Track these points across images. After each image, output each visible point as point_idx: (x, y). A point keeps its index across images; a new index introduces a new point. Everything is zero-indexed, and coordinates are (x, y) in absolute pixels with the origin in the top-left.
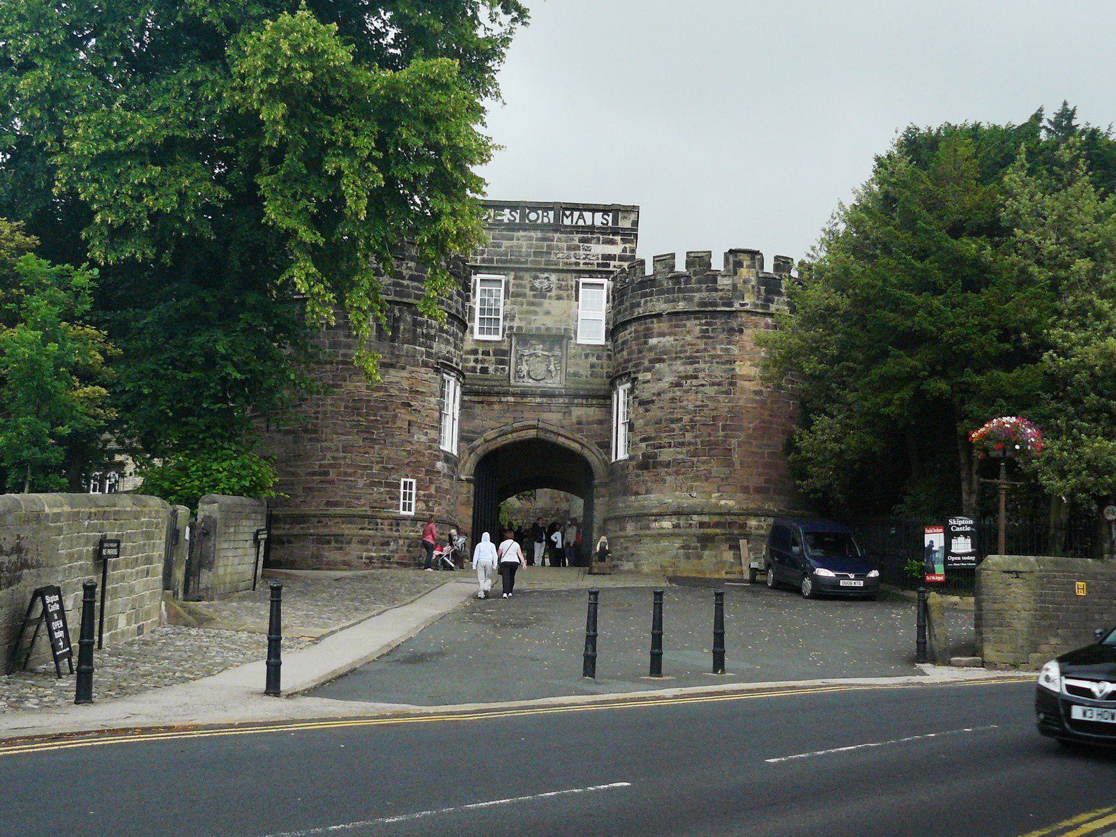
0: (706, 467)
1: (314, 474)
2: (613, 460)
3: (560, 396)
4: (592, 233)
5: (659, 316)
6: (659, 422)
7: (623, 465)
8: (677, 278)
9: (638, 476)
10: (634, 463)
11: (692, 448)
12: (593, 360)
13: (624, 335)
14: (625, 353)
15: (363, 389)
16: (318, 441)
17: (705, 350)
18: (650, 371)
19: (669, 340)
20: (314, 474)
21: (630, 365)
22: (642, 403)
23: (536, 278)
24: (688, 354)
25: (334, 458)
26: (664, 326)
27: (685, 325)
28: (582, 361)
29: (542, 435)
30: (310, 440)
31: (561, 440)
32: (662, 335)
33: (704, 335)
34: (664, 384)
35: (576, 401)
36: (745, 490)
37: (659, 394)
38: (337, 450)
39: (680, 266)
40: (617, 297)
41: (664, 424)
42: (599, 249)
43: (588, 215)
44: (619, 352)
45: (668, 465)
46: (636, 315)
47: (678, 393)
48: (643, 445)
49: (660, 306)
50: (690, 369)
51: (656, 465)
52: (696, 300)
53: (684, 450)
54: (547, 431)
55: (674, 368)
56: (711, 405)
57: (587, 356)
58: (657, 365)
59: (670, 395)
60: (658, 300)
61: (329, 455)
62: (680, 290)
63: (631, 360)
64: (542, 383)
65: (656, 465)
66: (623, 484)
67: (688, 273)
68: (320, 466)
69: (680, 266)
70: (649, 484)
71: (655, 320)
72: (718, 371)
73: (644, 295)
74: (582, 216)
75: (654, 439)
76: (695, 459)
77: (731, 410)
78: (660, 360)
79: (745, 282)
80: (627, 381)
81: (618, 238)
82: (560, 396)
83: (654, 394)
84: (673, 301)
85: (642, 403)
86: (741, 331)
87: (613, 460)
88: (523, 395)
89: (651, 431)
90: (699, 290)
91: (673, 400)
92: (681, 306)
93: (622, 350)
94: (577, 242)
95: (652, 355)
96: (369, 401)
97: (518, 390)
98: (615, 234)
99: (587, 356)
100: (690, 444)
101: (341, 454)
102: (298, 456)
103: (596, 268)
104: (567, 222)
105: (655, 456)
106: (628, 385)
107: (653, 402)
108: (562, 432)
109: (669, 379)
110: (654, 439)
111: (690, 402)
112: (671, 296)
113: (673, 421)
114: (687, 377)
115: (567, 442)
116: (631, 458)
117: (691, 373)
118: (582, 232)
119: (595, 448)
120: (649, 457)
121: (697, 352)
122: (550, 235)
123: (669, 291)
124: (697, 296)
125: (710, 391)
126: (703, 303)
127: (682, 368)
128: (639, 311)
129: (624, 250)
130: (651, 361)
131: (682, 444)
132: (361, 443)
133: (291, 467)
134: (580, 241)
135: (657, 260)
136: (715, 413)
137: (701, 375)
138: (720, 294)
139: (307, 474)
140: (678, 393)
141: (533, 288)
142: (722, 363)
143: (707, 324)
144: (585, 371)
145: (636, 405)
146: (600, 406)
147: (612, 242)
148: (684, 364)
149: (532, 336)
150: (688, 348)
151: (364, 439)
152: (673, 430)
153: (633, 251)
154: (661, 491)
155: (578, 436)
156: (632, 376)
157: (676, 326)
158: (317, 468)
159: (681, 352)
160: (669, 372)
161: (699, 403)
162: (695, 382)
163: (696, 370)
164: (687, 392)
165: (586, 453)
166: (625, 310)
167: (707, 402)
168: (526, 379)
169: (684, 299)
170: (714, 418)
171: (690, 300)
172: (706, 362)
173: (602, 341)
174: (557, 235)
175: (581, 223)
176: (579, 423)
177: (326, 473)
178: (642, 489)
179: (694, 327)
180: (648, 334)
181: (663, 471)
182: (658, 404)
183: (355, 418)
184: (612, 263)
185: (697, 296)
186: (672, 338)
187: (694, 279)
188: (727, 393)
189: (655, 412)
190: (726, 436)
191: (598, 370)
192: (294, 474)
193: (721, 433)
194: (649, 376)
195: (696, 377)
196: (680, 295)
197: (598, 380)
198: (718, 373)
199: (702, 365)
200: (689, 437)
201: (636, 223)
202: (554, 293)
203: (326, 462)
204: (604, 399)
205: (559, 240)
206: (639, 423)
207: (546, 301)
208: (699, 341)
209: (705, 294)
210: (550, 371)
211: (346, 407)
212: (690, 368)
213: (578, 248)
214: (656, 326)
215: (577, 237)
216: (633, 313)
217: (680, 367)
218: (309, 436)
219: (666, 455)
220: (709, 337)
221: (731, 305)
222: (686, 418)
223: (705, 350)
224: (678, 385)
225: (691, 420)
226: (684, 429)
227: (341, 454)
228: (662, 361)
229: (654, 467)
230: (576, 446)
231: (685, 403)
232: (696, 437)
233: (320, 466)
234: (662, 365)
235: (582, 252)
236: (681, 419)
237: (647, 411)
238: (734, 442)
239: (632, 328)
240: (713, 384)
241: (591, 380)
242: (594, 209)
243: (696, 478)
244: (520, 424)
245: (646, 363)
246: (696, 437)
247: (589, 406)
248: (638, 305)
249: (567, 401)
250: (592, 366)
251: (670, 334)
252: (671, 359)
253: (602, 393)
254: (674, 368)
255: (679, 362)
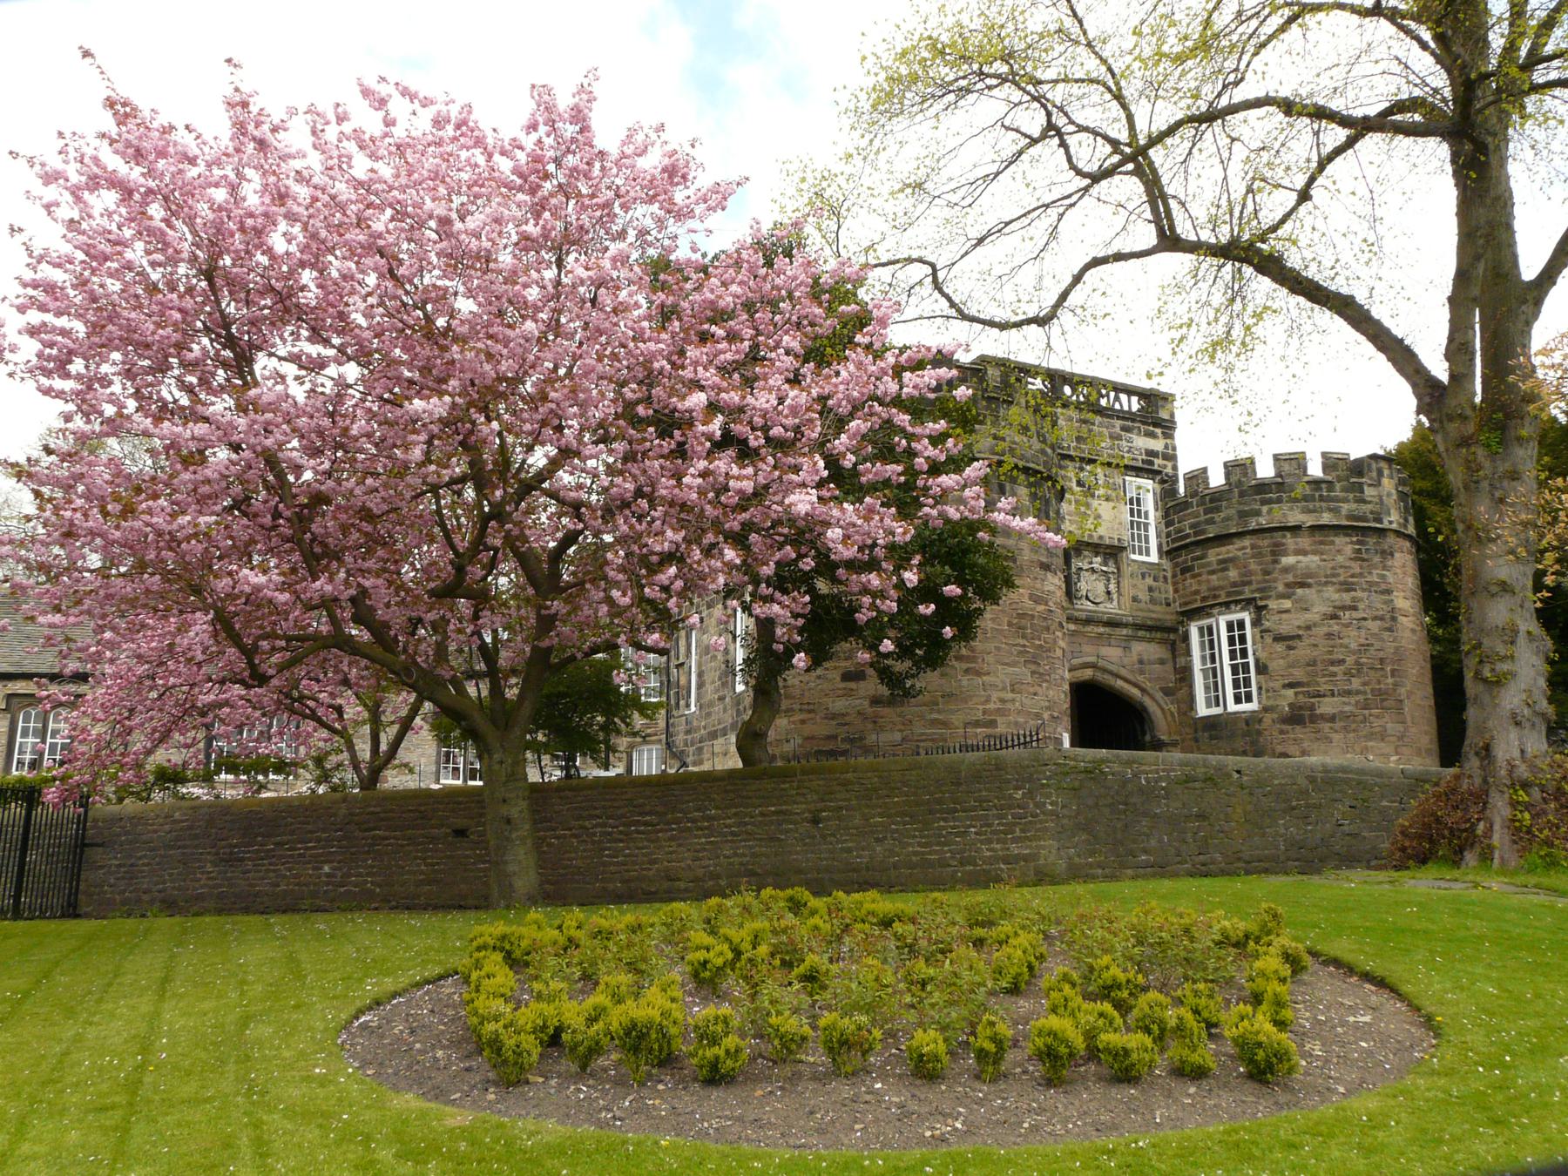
0: (1380, 722)
1: (977, 724)
2: (1202, 710)
3: (1126, 625)
4: (1133, 421)
5: (1296, 529)
6: (1312, 663)
7: (1251, 719)
8: (1316, 483)
9: (1282, 732)
10: (1275, 716)
11: (1361, 698)
12: (1149, 581)
13: (1214, 555)
14: (1233, 574)
15: (1026, 599)
16: (978, 674)
17: (1361, 575)
18: (1288, 597)
19: (1312, 560)
20: (977, 724)
21: (1246, 589)
22: (1278, 638)
23: (1082, 469)
24: (1342, 578)
25: (1003, 701)
26: (1304, 541)
27: (1333, 543)
28: (1139, 582)
29: (1100, 677)
30: (967, 671)
31: (1120, 683)
32: (1299, 552)
33: (1358, 557)
34: (1312, 616)
35: (1141, 633)
36: (1419, 752)
37: (1308, 628)
38: (1004, 689)
39: (1315, 469)
40: (1171, 505)
41: (1320, 667)
42: (1142, 442)
43: (1123, 397)
44: (1213, 572)
45: (1332, 719)
46: (1253, 525)
47: (1336, 628)
48: (1290, 692)
49: (1295, 517)
50: (1347, 598)
51: (1314, 718)
52: (1344, 512)
53: (1353, 700)
54: (1105, 670)
55: (1326, 595)
56: (1377, 645)
57: (1143, 577)
58: (1299, 591)
59: (1325, 629)
60: (1291, 509)
61: (995, 696)
62: (1322, 498)
63: (1249, 583)
64: (1101, 608)
65: (1314, 718)
66: (1253, 743)
67: (1329, 478)
68: (985, 712)
69: (1315, 469)
70: (1305, 744)
71: (1288, 535)
72: (1377, 600)
73: (1264, 502)
74: (1117, 399)
75: (1308, 684)
76: (1366, 712)
77: (1397, 648)
78: (1303, 585)
79: (1389, 495)
80: (1243, 609)
81: (1158, 431)
82: (1126, 625)
83: (1299, 627)
84: (1314, 511)
85: (1278, 638)
86: (1392, 554)
87: (1202, 710)
88: (1088, 621)
89: (1299, 674)
90: (1346, 500)
91: (1329, 636)
92: (1326, 519)
93: (1226, 569)
94: (1118, 429)
95: (1290, 578)
96: (1033, 617)
97: (1083, 615)
98: (1155, 425)
99: (1143, 577)
100: (1358, 692)
101: (1010, 696)
102: (948, 696)
103: (1140, 464)
104: (1103, 402)
105: (1312, 708)
106: (1246, 617)
107: (1299, 637)
108: (1123, 672)
109: (1319, 609)
110: (1308, 684)
111: (1353, 639)
112: (1311, 505)
113: (1333, 663)
114: (1344, 608)
115: (1126, 686)
116: (1266, 709)
117: (1348, 603)
118: (1124, 418)
119: (1159, 695)
120: (1301, 708)
121: (1353, 576)
122: (1090, 416)
123: (1306, 498)
124: (1345, 508)
125: (1374, 626)
126: (1350, 517)
127: (1336, 596)
128: (1263, 520)
129: (1166, 447)
130: (1287, 585)
131: (1349, 693)
132: (1029, 679)
133: (939, 712)
134: (1124, 429)
135: (1277, 458)
136: (1381, 654)
137: (1361, 606)
138: (1370, 507)
139: (966, 725)
140: (1336, 628)
141: (1079, 483)
142: (1382, 593)
143: (1359, 542)
144: (1144, 596)
145: (1269, 640)
146: (1162, 642)
147: (1152, 435)
148: (1339, 591)
149: (1088, 544)
150: (1341, 571)
151: (1033, 673)
152: (1334, 674)
153: (1174, 449)
154: (1326, 753)
155: (1140, 678)
156: (1260, 603)
157: (1322, 543)
158: (980, 716)
159: (1334, 575)
160: (1320, 601)
161: (1362, 641)
162: (1355, 615)
163: (1354, 600)
164: (1347, 626)
165: (1147, 701)
166: (1228, 519)
167: (1371, 641)
168: (1084, 601)
169: (1330, 510)
170: (1382, 661)
171: (1335, 511)
172: (1364, 590)
173: (1154, 558)
174: (1098, 419)
175: (1117, 406)
176: (1141, 662)
177: (993, 724)
178: (1292, 749)
179: (1345, 546)
180: (1278, 551)
181: (1326, 726)
182: (1307, 641)
183: (1022, 642)
184: (1157, 461)
185: (1345, 508)
186: (1316, 558)
187: (1338, 486)
188: (1390, 630)
189: (1303, 651)
190: (1396, 685)
191: (1156, 594)
192: (945, 724)
193: (1390, 680)
194: (1287, 604)
195: (1355, 608)
196: (1324, 505)
197: (1157, 608)
198: (1379, 606)
199: (1359, 594)
200: (1356, 683)
201: (1172, 415)
202: (1101, 492)
203: (991, 706)
204: (1171, 636)
205: (1101, 425)
206: (1275, 665)
207: (1095, 503)
208: (1353, 564)
209: (1354, 506)
210: (1108, 593)
211: (1010, 624)
212: (1347, 598)
213: (1119, 438)
214: (1289, 541)
215: (1118, 423)
216: (1246, 525)
217: (1331, 593)
218: (965, 666)
219: (1327, 706)
220: (1364, 560)
221: (1380, 521)
222: (1350, 660)
223: (1361, 575)
224: (1334, 617)
225: (1357, 663)
226: (1348, 673)
227: (1010, 696)
228: (1309, 586)
229: (1312, 722)
230: (1135, 692)
231: (1345, 641)
232: (1365, 684)
233: (985, 712)
234: (1307, 591)
235: (1124, 443)
236: (1342, 662)
237: (1290, 648)
238: (1403, 691)
239: (1247, 542)
240: (1375, 618)
241: (1151, 607)
242: (1130, 391)
243: (1371, 736)
244: (1079, 661)
245: (1281, 588)
246: (1365, 684)
247: (1151, 640)
248: (1258, 513)
249: (1130, 632)
250: (1151, 589)
251: (1315, 553)
252: (1319, 584)
253: (1168, 624)
254: (1326, 595)
255: (1331, 588)
